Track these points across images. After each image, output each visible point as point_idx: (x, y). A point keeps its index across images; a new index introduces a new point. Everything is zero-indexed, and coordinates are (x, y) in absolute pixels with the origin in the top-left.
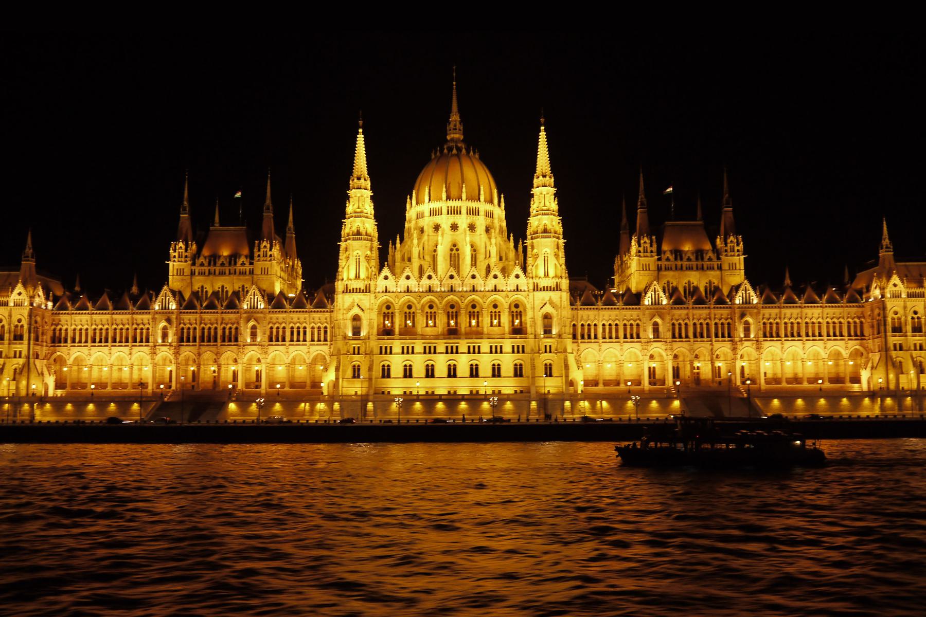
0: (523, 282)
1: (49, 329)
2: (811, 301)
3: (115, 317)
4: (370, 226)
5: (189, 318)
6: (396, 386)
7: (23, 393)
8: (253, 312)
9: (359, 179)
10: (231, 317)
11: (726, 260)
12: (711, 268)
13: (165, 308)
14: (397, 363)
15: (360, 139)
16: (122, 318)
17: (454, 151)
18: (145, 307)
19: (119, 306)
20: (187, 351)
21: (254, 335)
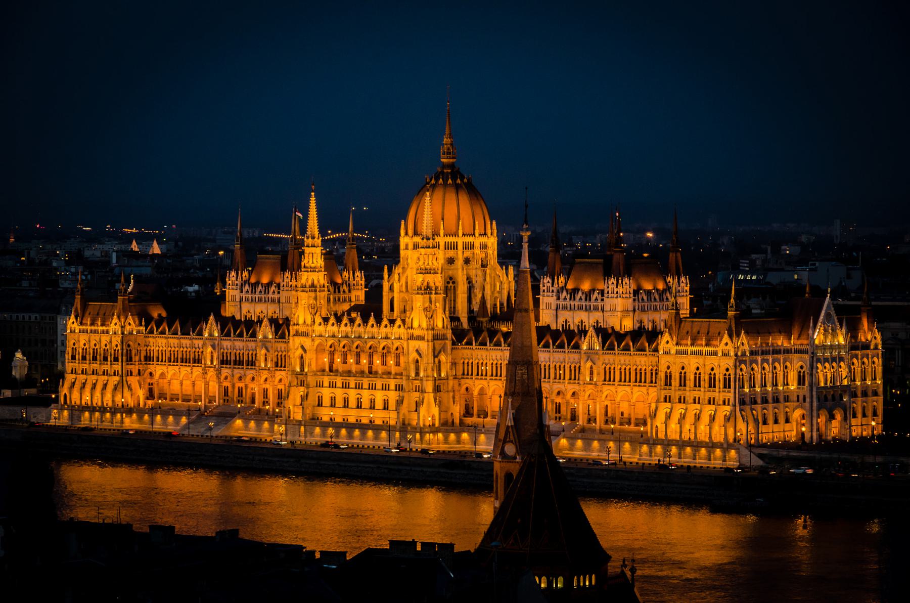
0: (402, 330)
1: (143, 349)
2: (642, 349)
3: (182, 341)
4: (320, 278)
5: (226, 344)
6: (326, 414)
7: (120, 405)
8: (265, 342)
9: (308, 238)
10: (252, 345)
11: (608, 303)
12: (596, 309)
13: (211, 335)
14: (326, 393)
15: (313, 200)
16: (186, 342)
17: (433, 182)
18: (200, 334)
19: (185, 333)
20: (226, 372)
21: (266, 360)
